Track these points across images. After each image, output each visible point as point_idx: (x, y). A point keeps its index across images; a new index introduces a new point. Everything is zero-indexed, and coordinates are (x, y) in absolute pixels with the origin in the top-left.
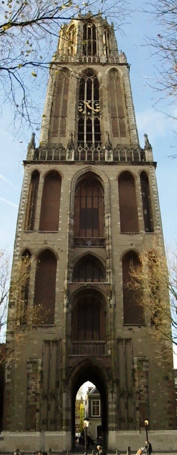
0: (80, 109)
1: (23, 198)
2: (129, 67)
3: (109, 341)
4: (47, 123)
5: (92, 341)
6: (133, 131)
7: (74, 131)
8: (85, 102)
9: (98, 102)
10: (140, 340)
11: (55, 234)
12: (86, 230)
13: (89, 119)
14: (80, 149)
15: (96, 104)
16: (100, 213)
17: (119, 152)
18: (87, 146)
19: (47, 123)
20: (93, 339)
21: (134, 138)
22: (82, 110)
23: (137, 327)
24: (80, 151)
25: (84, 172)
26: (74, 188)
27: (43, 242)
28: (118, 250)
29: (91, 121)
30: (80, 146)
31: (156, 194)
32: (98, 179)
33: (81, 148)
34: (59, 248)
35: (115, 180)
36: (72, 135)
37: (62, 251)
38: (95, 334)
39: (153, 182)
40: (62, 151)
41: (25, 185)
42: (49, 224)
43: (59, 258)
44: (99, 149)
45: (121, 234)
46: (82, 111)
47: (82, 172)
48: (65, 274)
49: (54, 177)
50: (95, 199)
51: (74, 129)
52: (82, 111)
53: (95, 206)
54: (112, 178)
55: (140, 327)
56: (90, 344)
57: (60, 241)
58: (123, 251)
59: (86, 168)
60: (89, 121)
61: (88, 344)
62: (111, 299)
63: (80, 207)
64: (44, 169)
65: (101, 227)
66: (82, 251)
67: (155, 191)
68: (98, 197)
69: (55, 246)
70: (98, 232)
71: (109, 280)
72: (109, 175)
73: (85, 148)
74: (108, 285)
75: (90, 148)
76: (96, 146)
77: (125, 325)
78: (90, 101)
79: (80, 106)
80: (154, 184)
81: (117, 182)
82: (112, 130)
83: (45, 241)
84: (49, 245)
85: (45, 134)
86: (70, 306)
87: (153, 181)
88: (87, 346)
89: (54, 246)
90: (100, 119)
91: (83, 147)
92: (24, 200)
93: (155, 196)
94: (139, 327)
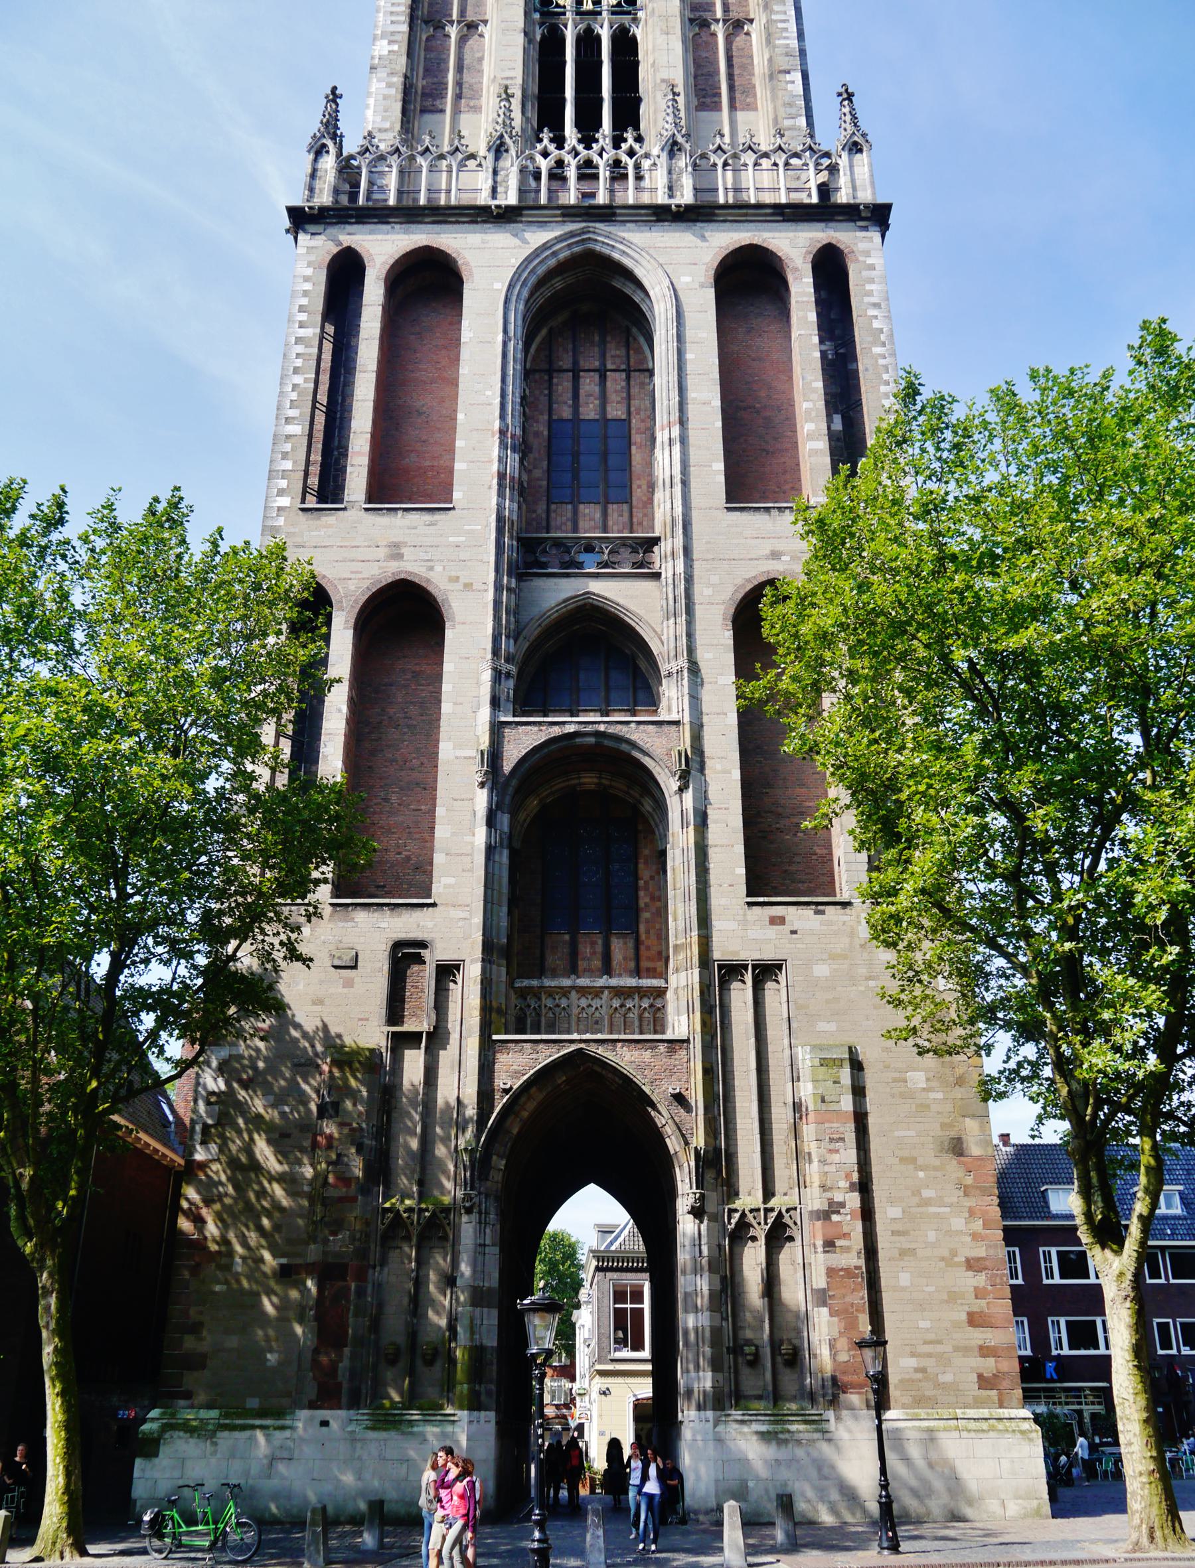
1: (296, 371)
3: (683, 974)
4: (395, 47)
5: (602, 982)
6: (788, 77)
7: (520, 81)
10: (822, 970)
11: (438, 517)
12: (575, 512)
13: (589, 31)
14: (545, 154)
16: (636, 438)
17: (720, 163)
18: (574, 142)
19: (395, 47)
20: (607, 970)
21: (793, 111)
23: (809, 912)
24: (544, 165)
25: (562, 256)
26: (520, 322)
27: (382, 553)
28: (715, 579)
29: (598, 39)
30: (546, 141)
31: (884, 344)
32: (629, 289)
33: (552, 147)
34: (453, 574)
35: (702, 286)
36: (509, 97)
37: (468, 586)
38: (620, 949)
39: (870, 293)
40: (462, 165)
41: (303, 317)
42: (406, 477)
44: (631, 153)
47: (554, 254)
48: (478, 684)
49: (429, 284)
50: (615, 382)
51: (518, 73)
53: (615, 411)
54: (687, 279)
55: (823, 913)
56: (597, 992)
57: (457, 550)
58: (739, 581)
59: (572, 234)
60: (588, 42)
61: (583, 991)
62: (687, 787)
63: (550, 414)
64: (382, 248)
65: (638, 493)
66: (557, 592)
67: (881, 330)
68: (628, 372)
69: (438, 568)
70: (626, 514)
71: (673, 698)
72: (675, 273)
73: (567, 148)
74: (674, 728)
75: (588, 147)
76: (617, 142)
77: (750, 899)
80: (874, 300)
81: (711, 293)
82: (691, 80)
83: (397, 545)
84: (412, 567)
85: (385, 97)
86: (504, 820)
87: (868, 287)
88: (584, 1002)
89: (431, 569)
90: (638, 32)
91: (560, 147)
92: (298, 379)
93: (877, 350)
94: (817, 912)
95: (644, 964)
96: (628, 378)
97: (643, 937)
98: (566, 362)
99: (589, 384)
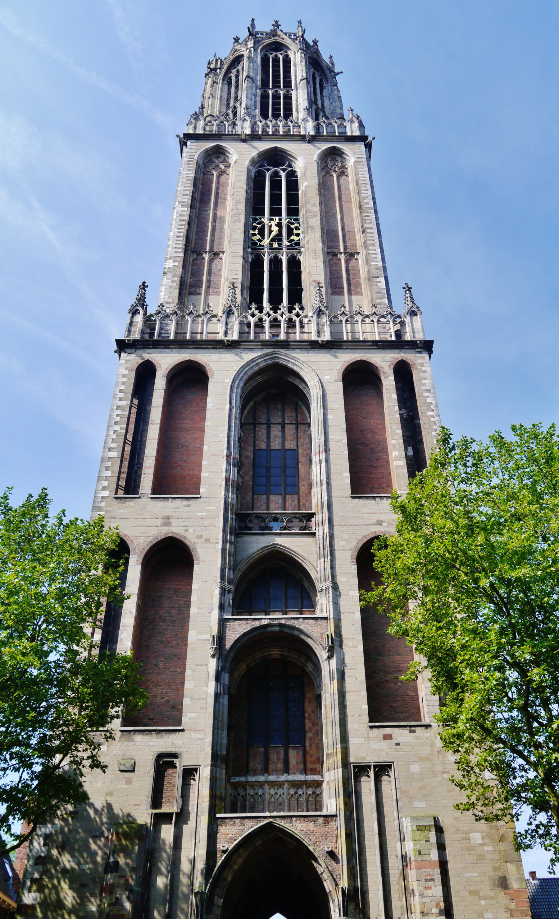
0: (254, 235)
1: (116, 423)
2: (368, 146)
3: (332, 772)
4: (177, 264)
5: (283, 778)
6: (378, 280)
7: (240, 280)
8: (265, 220)
9: (297, 220)
10: (415, 768)
11: (191, 502)
12: (268, 499)
13: (276, 257)
14: (253, 315)
15: (293, 224)
16: (301, 459)
17: (344, 320)
18: (268, 309)
19: (177, 264)
20: (287, 770)
21: (381, 295)
22: (258, 237)
23: (406, 731)
24: (252, 320)
25: (261, 365)
26: (238, 399)
27: (159, 522)
28: (346, 536)
29: (281, 261)
30: (253, 309)
31: (433, 411)
32: (297, 382)
33: (256, 312)
34: (199, 534)
35: (336, 381)
36: (234, 288)
37: (207, 541)
38: (294, 757)
39: (424, 385)
40: (209, 320)
41: (122, 395)
42: (174, 481)
43: (199, 560)
44: (298, 315)
45: (353, 498)
46: (260, 240)
47: (257, 364)
48: (212, 596)
49: (190, 380)
50: (290, 430)
52: (260, 240)
53: (290, 445)
54: (328, 377)
55: (414, 732)
56: (280, 785)
57: (201, 521)
58: (359, 537)
59: (267, 355)
60: (275, 263)
61: (272, 784)
62: (332, 656)
63: (254, 445)
64: (165, 361)
65: (303, 489)
66: (257, 544)
67: (431, 403)
68: (297, 424)
69: (191, 530)
70: (296, 501)
71: (324, 604)
72: (321, 375)
73: (264, 312)
74: (324, 621)
75: (275, 312)
76: (290, 310)
77: (371, 724)
78: (277, 218)
79: (254, 228)
80: (427, 388)
81: (340, 384)
82: (328, 281)
83: (168, 518)
84: (176, 529)
85: (170, 287)
86: (226, 677)
87: (423, 381)
88: (272, 791)
89: (187, 531)
90: (301, 258)
91: (261, 312)
92: (117, 428)
93: (430, 413)
94: (411, 732)
95: (309, 766)
96: (297, 428)
97: (308, 749)
98: (263, 420)
99: (276, 431)
